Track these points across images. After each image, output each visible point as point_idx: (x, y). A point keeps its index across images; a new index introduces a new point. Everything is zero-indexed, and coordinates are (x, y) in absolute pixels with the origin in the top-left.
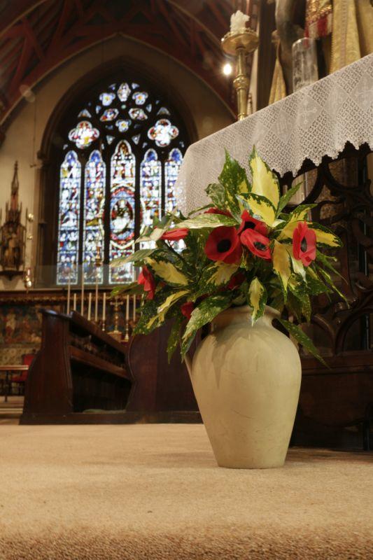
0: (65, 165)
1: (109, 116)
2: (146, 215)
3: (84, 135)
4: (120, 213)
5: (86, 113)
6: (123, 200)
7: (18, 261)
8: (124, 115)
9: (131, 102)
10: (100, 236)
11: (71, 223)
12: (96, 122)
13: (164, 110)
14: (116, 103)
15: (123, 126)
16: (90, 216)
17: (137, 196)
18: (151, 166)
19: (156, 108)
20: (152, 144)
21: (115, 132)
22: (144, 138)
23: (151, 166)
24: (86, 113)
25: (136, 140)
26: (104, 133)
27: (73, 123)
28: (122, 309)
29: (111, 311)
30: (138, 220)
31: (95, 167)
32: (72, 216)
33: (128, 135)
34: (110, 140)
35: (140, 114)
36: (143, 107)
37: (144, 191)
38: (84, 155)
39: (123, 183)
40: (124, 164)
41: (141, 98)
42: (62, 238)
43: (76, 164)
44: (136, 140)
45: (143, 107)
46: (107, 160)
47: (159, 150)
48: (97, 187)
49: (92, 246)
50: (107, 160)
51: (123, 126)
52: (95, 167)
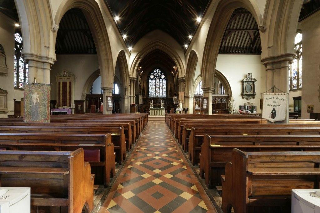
0: (149, 81)
1: (155, 74)
2: (160, 88)
3: (152, 76)
4: (157, 88)
5: (152, 73)
6: (157, 86)
7: (145, 94)
8: (157, 74)
9: (158, 72)
10: (154, 91)
11: (150, 89)
12: (153, 75)
13: (163, 73)
14: (156, 72)
15: (157, 75)
16: (153, 88)
17: (159, 85)
18: (161, 81)
19: (162, 73)
20: (161, 78)
21: (156, 76)
22: (160, 77)
23: (161, 81)
24: (152, 73)
25: (159, 77)
26: (155, 76)
27: (150, 75)
28: (158, 101)
29: (157, 101)
30: (159, 88)
31: (154, 81)
32: (151, 88)
33: (158, 77)
34: (156, 77)
35: (159, 74)
36: (160, 73)
37: (160, 85)
38: (152, 80)
39: (157, 83)
40: (157, 81)
41: (160, 71)
42: (149, 91)
43: (151, 81)
44: (159, 77)
45: (160, 73)
46: (155, 80)
47: (162, 79)
48: (154, 84)
49: (154, 92)
50: (155, 80)
51: (157, 75)
52: (154, 81)
